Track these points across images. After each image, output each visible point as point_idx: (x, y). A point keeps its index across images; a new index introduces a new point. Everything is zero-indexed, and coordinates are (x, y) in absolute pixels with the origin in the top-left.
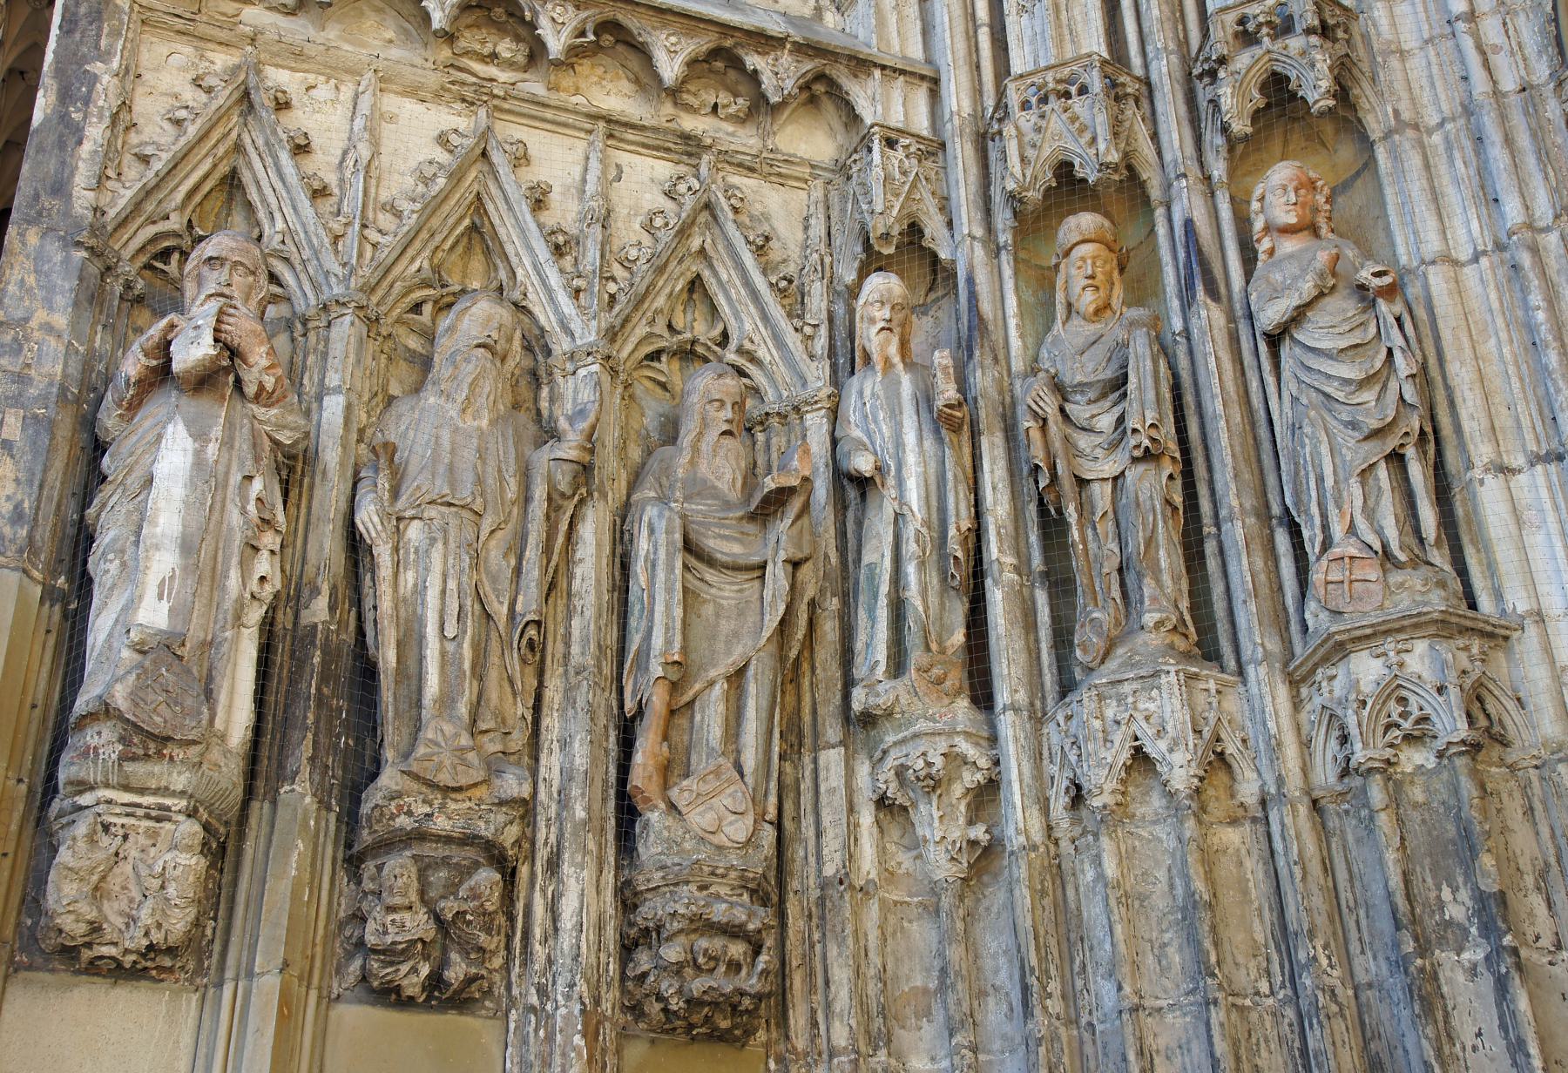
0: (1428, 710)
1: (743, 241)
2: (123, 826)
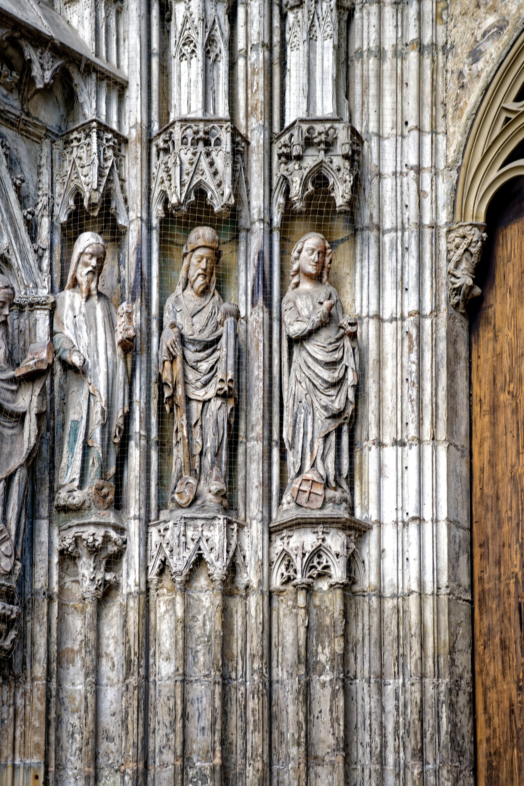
0: (330, 563)
1: (10, 181)
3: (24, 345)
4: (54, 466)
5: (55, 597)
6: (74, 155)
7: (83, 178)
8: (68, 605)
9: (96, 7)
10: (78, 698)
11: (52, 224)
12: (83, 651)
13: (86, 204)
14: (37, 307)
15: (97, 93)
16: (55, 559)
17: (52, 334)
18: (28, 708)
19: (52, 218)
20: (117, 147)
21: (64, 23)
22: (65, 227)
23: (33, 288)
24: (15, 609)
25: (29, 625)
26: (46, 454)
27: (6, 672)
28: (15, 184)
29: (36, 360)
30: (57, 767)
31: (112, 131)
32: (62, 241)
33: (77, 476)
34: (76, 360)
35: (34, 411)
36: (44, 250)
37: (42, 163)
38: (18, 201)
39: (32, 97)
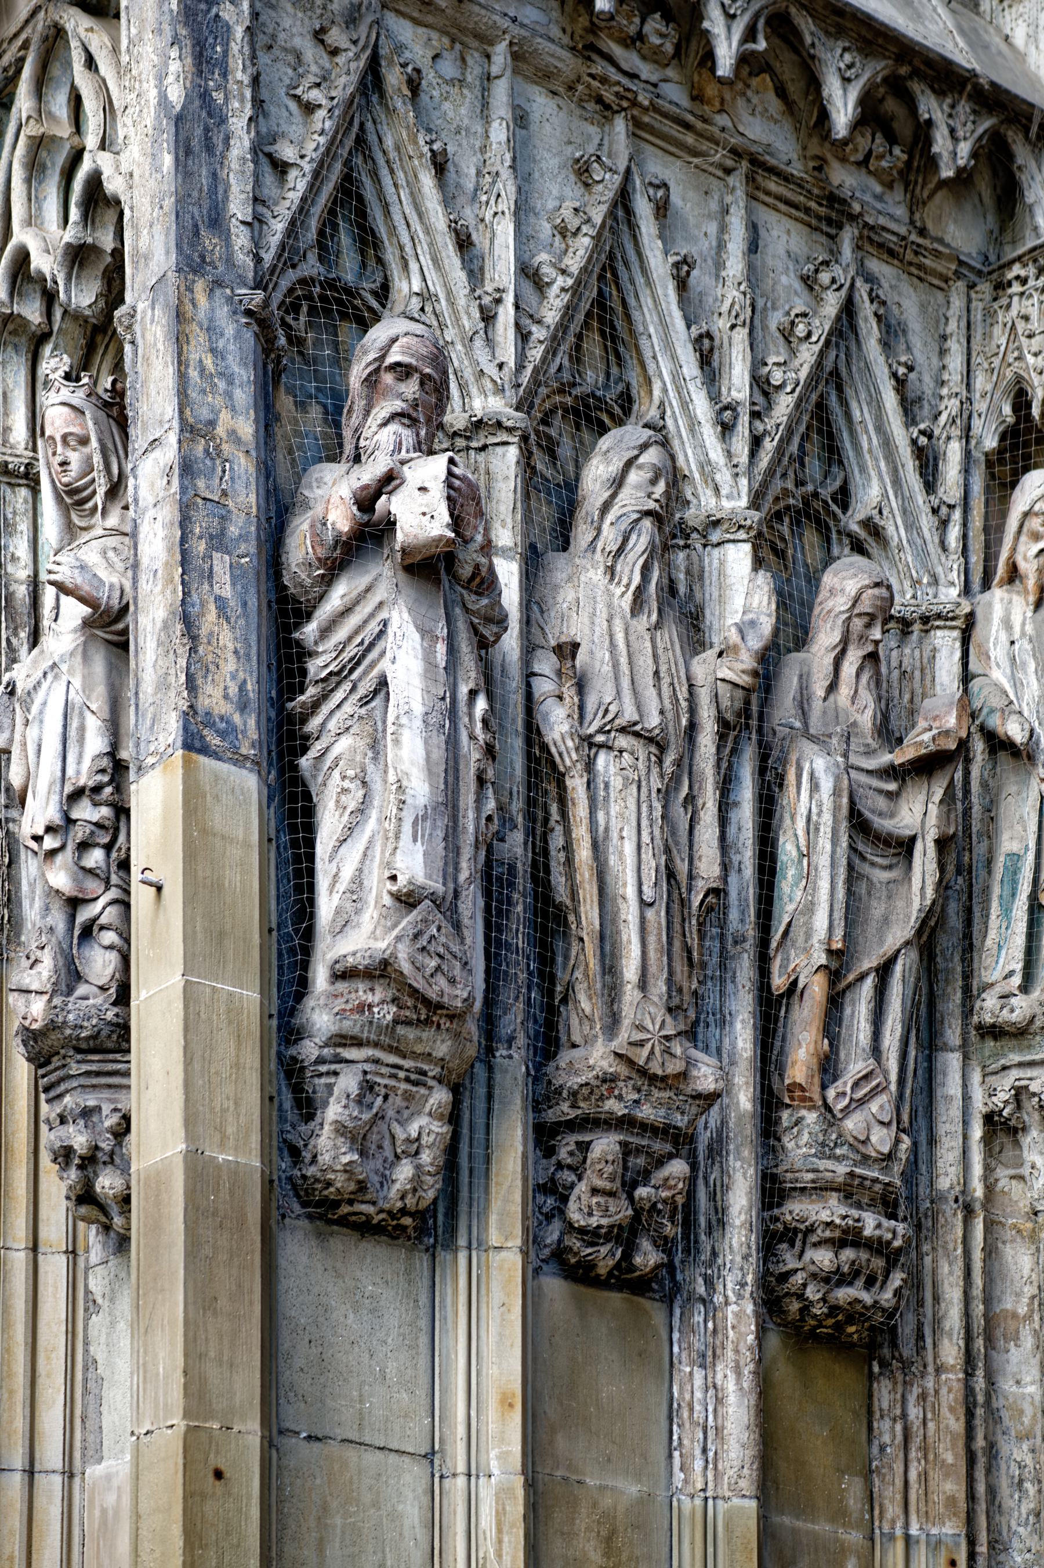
1: (886, 370)
2: (386, 1086)
3: (912, 701)
4: (971, 945)
5: (977, 1206)
6: (1014, 312)
7: (1030, 359)
8: (1004, 1225)
10: (1029, 1411)
11: (967, 454)
12: (1036, 1318)
14: (937, 623)
16: (977, 1132)
17: (966, 677)
18: (931, 1425)
19: (967, 442)
21: (997, 41)
22: (992, 461)
23: (929, 584)
24: (901, 1228)
25: (928, 1260)
26: (955, 921)
27: (886, 1352)
28: (894, 375)
29: (935, 732)
30: (992, 1544)
32: (988, 490)
33: (1019, 966)
34: (1015, 731)
35: (932, 834)
36: (951, 507)
37: (949, 330)
38: (900, 410)
39: (931, 196)
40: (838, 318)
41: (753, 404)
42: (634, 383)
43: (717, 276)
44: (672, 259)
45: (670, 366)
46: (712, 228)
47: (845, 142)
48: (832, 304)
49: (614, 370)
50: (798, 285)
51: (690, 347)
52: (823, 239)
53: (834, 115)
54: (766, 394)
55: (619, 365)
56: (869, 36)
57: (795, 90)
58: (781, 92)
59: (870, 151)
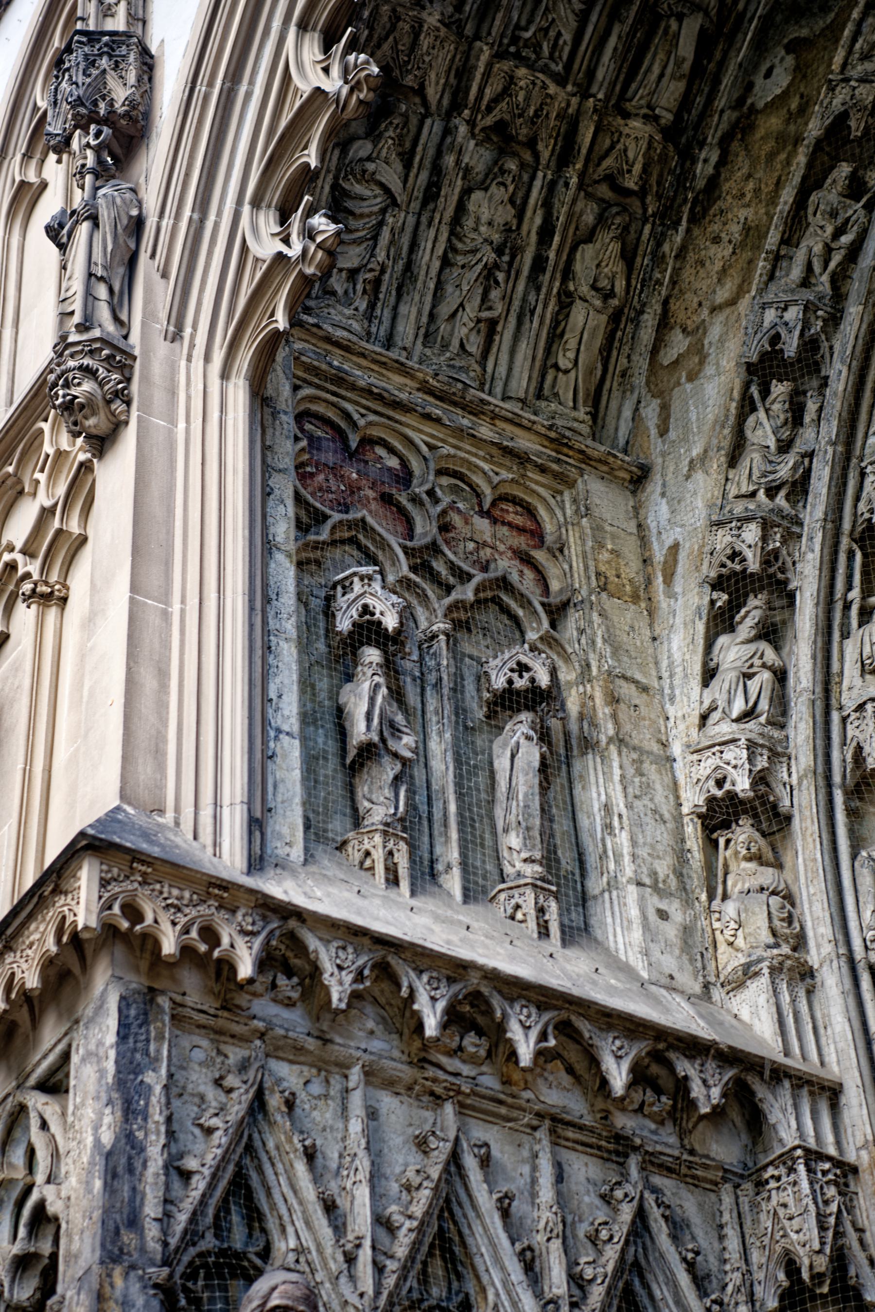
1: (677, 1257)
6: (774, 1202)
9: (775, 991)
13: (805, 1275)
15: (796, 1106)
19: (753, 1305)
20: (842, 1181)
21: (729, 1019)
28: (684, 1260)
31: (829, 1158)
37: (724, 1220)
38: (693, 1286)
39: (694, 1127)
40: (633, 1222)
41: (571, 1296)
42: (472, 1292)
43: (533, 1203)
44: (495, 1196)
45: (500, 1275)
46: (526, 1169)
47: (623, 1099)
48: (627, 1212)
49: (455, 1285)
50: (598, 1202)
51: (515, 1259)
52: (614, 1166)
53: (612, 1081)
54: (581, 1288)
55: (459, 1280)
56: (632, 1027)
57: (580, 1067)
58: (570, 1070)
59: (643, 1102)
